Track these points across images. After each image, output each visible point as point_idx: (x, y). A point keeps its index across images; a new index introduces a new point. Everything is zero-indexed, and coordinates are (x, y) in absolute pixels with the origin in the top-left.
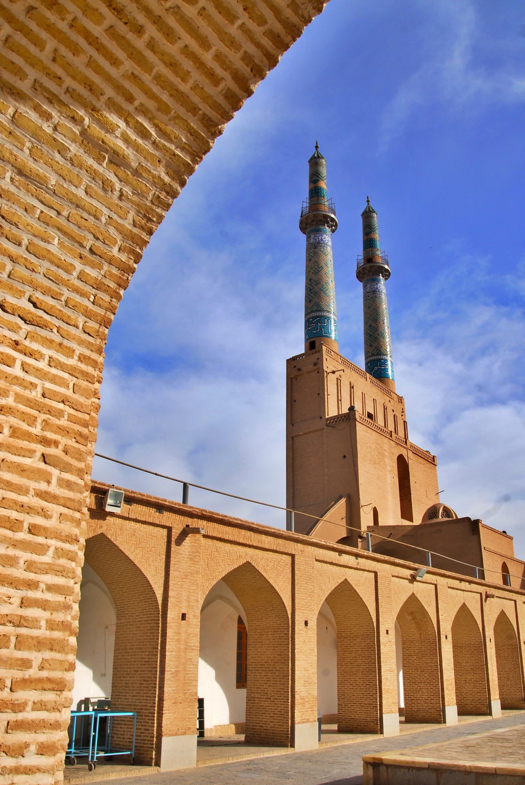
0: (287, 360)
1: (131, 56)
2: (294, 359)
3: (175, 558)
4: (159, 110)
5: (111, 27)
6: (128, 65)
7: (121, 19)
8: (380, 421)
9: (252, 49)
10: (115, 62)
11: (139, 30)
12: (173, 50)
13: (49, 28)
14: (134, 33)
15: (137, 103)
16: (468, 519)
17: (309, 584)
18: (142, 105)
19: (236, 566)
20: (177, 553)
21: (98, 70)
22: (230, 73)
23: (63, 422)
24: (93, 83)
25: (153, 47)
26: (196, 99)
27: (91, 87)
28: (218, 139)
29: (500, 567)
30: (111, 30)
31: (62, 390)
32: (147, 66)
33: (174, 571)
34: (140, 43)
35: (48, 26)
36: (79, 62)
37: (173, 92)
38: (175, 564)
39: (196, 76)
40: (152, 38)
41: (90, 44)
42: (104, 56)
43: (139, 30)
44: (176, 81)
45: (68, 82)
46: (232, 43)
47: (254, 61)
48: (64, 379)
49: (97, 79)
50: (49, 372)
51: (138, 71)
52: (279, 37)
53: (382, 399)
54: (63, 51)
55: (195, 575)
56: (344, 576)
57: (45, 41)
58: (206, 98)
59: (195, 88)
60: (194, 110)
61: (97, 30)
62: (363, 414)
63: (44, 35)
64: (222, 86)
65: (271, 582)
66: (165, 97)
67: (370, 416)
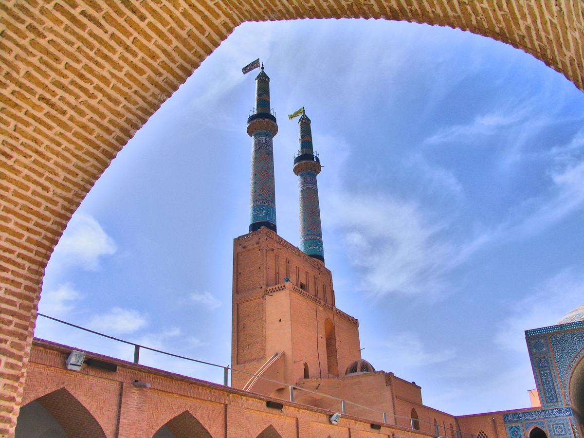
0: (234, 239)
1: (59, 125)
2: (239, 238)
3: (125, 408)
4: (76, 148)
5: (48, 112)
6: (58, 129)
7: (54, 109)
8: (312, 292)
9: (130, 116)
10: (50, 128)
11: (64, 113)
12: (84, 120)
13: (13, 116)
14: (61, 114)
15: (63, 147)
16: (383, 372)
17: (239, 429)
18: (66, 147)
19: (176, 415)
20: (127, 404)
21: (40, 132)
22: (118, 128)
23: (12, 328)
24: (37, 139)
25: (72, 119)
26: (98, 142)
27: (36, 141)
28: (113, 161)
29: (410, 412)
30: (48, 114)
31: (12, 308)
32: (69, 129)
33: (124, 419)
34: (65, 119)
35: (12, 115)
36: (29, 130)
37: (85, 140)
38: (124, 413)
39: (98, 131)
40: (72, 115)
41: (36, 121)
42: (44, 126)
43: (64, 113)
44: (86, 134)
45: (23, 140)
46: (119, 114)
47: (132, 122)
48: (14, 301)
49: (39, 137)
50: (4, 298)
51: (63, 131)
52: (146, 109)
53: (313, 273)
54: (20, 125)
55: (141, 423)
56: (269, 422)
57: (10, 122)
58: (105, 141)
59: (98, 137)
60: (97, 147)
61: (40, 115)
62: (297, 284)
63: (9, 119)
64: (114, 134)
65: (206, 427)
66: (80, 142)
67: (302, 286)
